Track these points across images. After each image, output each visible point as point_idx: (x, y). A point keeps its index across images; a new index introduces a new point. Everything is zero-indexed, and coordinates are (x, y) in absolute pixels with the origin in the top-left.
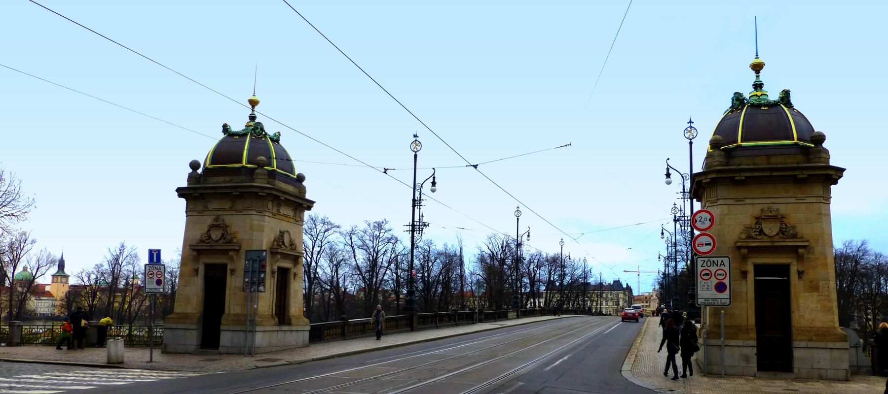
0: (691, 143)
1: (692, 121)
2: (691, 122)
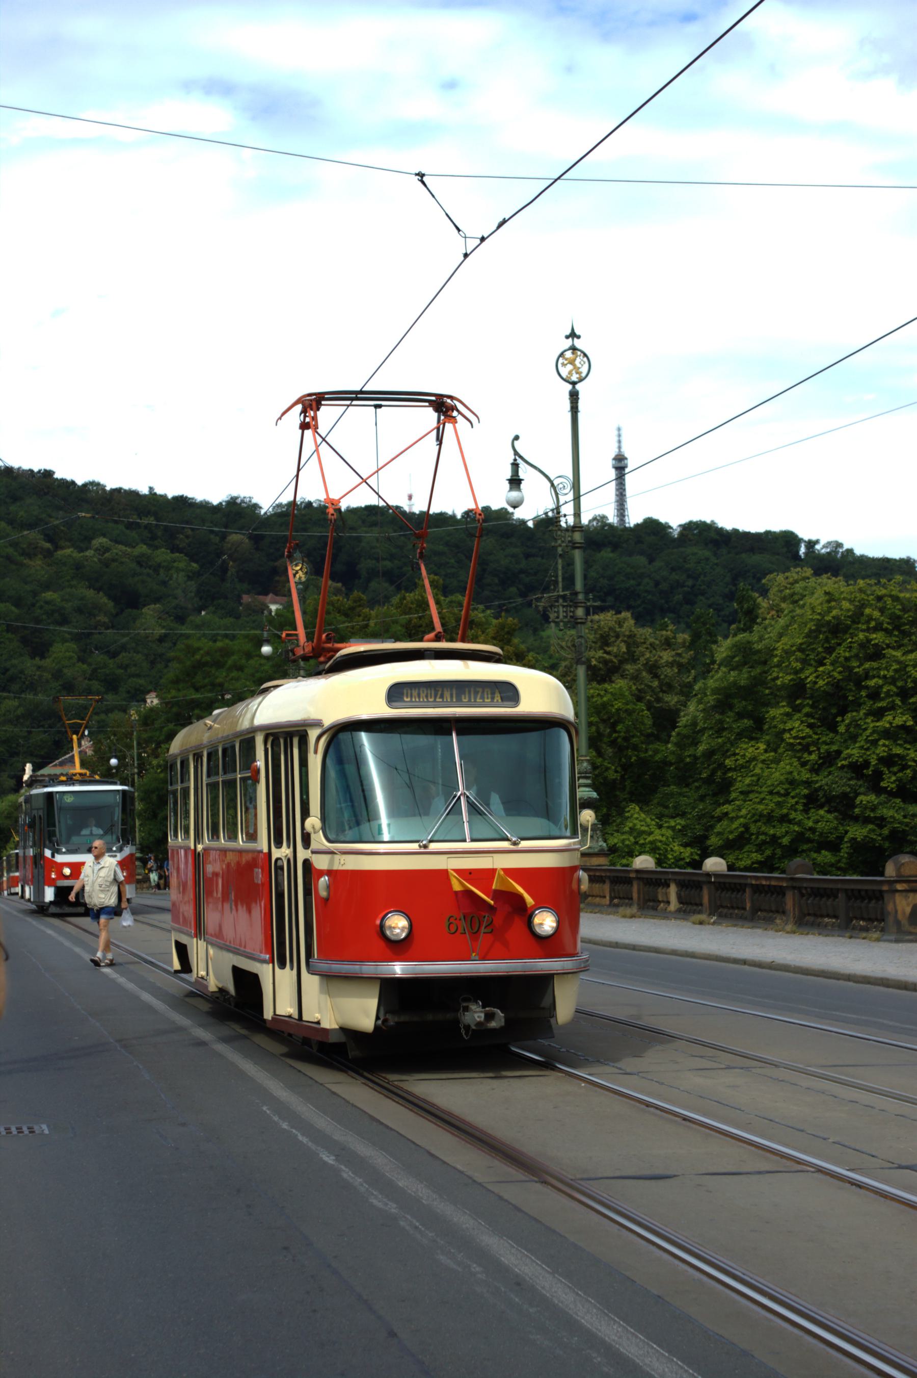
0: (574, 396)
1: (577, 333)
2: (573, 335)
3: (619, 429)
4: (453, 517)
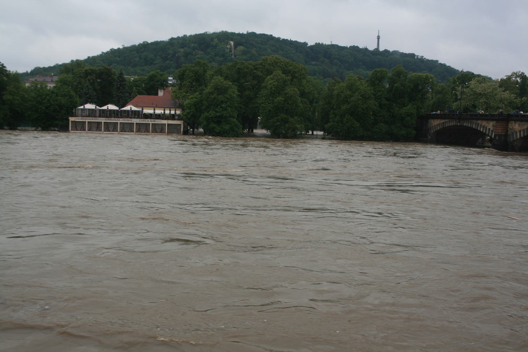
3: (379, 31)
4: (347, 47)
